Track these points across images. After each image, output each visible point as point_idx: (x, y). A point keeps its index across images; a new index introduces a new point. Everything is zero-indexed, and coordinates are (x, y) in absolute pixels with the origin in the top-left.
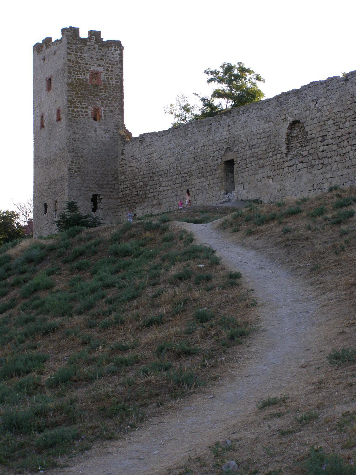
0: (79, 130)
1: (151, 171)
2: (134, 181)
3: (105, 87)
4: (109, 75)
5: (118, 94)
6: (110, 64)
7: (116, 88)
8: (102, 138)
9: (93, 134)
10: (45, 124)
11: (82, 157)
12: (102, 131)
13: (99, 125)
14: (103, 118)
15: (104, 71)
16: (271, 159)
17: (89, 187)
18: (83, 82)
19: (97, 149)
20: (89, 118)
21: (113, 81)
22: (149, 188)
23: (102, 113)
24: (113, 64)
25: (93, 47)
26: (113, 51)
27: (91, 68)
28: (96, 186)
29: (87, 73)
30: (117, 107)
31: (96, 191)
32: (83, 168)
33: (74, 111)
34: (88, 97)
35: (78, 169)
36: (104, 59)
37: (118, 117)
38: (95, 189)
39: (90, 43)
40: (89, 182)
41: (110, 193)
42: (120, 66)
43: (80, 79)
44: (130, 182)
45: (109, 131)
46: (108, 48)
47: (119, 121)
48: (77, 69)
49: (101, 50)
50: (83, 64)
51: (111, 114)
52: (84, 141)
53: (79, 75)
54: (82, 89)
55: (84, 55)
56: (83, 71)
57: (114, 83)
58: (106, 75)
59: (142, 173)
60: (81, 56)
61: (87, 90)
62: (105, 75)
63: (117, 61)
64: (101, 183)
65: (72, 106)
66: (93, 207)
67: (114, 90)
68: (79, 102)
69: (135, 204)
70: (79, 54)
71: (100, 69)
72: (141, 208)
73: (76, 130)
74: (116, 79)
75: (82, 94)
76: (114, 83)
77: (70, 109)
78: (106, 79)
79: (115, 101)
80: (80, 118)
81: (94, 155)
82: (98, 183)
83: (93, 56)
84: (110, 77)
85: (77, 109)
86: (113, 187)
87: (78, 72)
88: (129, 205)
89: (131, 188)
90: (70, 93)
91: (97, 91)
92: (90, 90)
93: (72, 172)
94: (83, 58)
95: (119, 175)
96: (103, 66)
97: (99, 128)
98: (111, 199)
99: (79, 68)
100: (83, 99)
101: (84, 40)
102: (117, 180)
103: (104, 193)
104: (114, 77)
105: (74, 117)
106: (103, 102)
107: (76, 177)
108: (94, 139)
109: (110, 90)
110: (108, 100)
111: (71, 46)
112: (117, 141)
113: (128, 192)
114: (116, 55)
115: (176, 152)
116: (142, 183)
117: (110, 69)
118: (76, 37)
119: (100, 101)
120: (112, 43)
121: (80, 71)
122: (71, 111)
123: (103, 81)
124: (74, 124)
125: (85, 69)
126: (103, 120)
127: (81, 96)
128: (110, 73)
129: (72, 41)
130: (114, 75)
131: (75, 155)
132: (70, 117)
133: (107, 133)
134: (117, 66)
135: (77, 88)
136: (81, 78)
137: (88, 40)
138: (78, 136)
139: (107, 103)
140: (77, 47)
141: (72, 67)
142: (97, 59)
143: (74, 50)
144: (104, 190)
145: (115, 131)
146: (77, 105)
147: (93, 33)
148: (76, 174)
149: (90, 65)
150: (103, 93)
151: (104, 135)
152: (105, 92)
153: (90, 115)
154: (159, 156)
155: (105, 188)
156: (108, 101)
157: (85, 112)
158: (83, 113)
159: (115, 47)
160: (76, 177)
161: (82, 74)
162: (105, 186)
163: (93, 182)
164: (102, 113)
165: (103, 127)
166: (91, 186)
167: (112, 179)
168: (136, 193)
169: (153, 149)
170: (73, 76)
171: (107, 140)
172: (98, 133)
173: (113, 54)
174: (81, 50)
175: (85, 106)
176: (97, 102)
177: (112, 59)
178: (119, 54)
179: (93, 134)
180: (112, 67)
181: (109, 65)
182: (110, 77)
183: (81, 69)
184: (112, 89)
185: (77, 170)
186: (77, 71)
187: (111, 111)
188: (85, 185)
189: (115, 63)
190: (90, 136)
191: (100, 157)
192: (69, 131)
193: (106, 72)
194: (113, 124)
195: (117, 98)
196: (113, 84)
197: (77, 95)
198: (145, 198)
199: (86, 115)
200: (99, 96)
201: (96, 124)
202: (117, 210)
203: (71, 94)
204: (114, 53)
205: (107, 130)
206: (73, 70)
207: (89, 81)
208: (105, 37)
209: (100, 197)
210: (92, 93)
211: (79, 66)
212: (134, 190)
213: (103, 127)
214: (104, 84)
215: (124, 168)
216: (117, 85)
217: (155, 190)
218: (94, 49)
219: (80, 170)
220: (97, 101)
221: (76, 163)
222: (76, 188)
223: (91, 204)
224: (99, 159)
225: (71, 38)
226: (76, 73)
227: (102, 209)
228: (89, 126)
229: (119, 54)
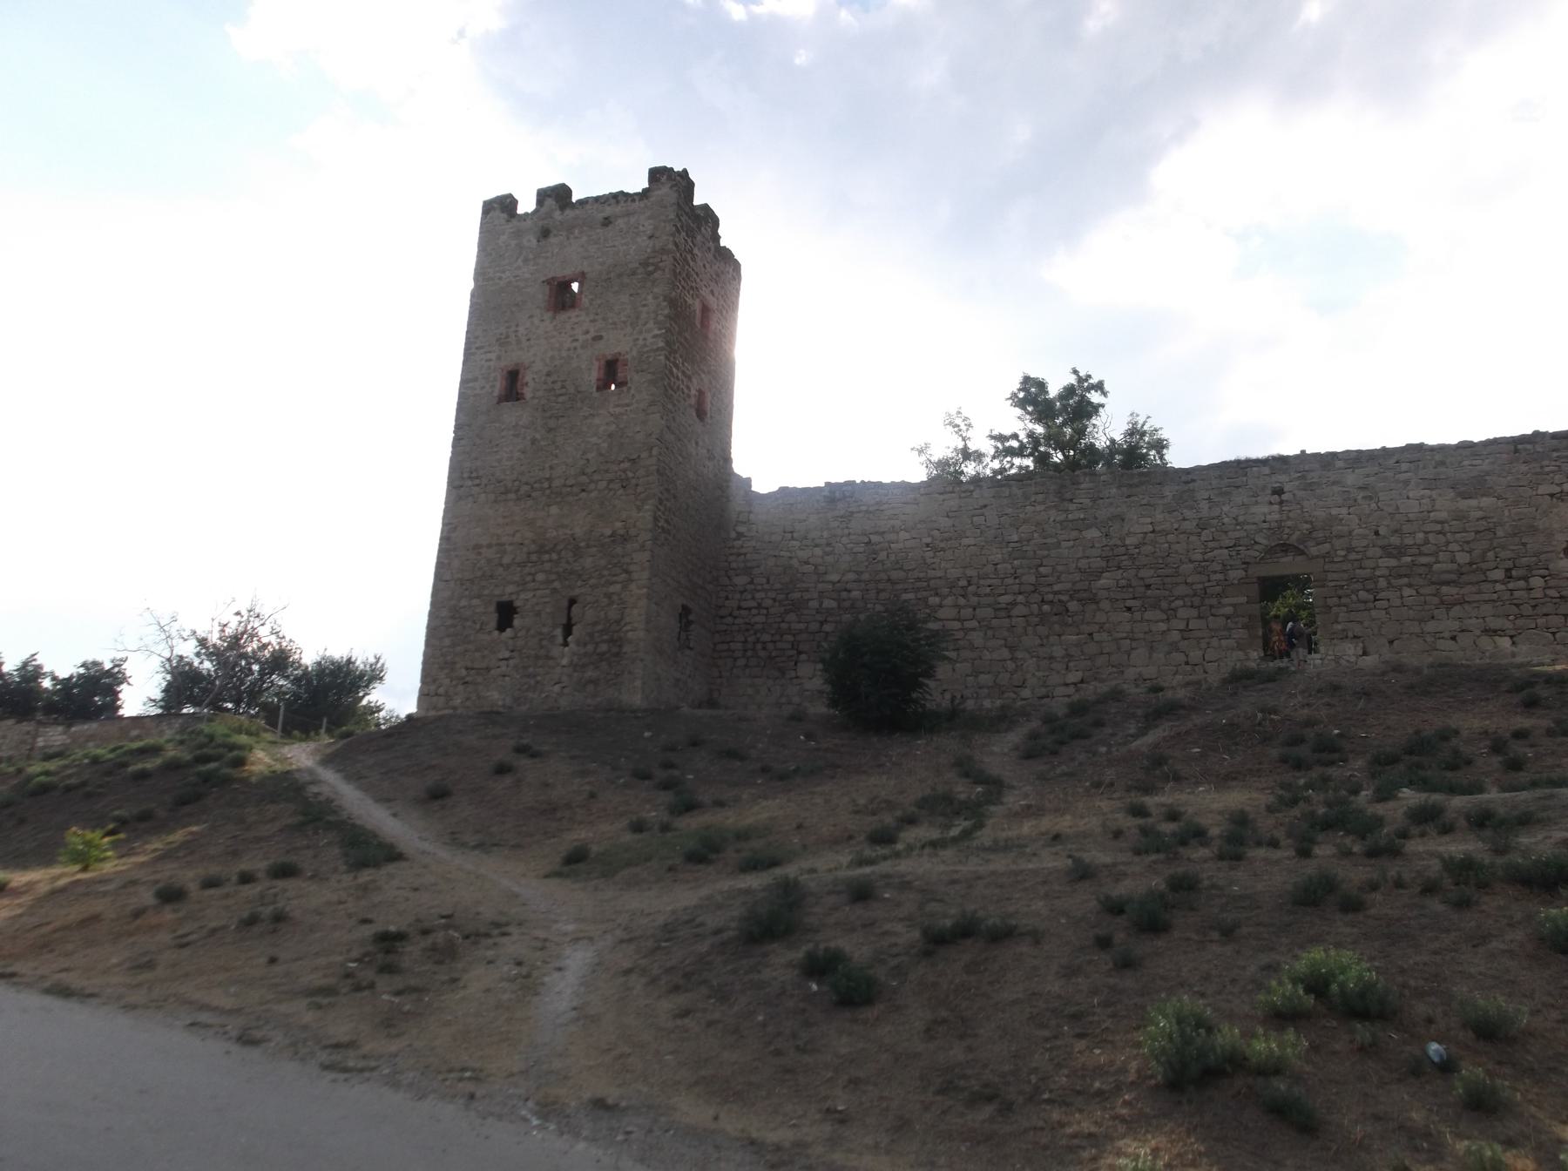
10: (528, 393)
16: (1499, 587)
88: (762, 654)
115: (1015, 538)
154: (929, 540)
212: (792, 617)
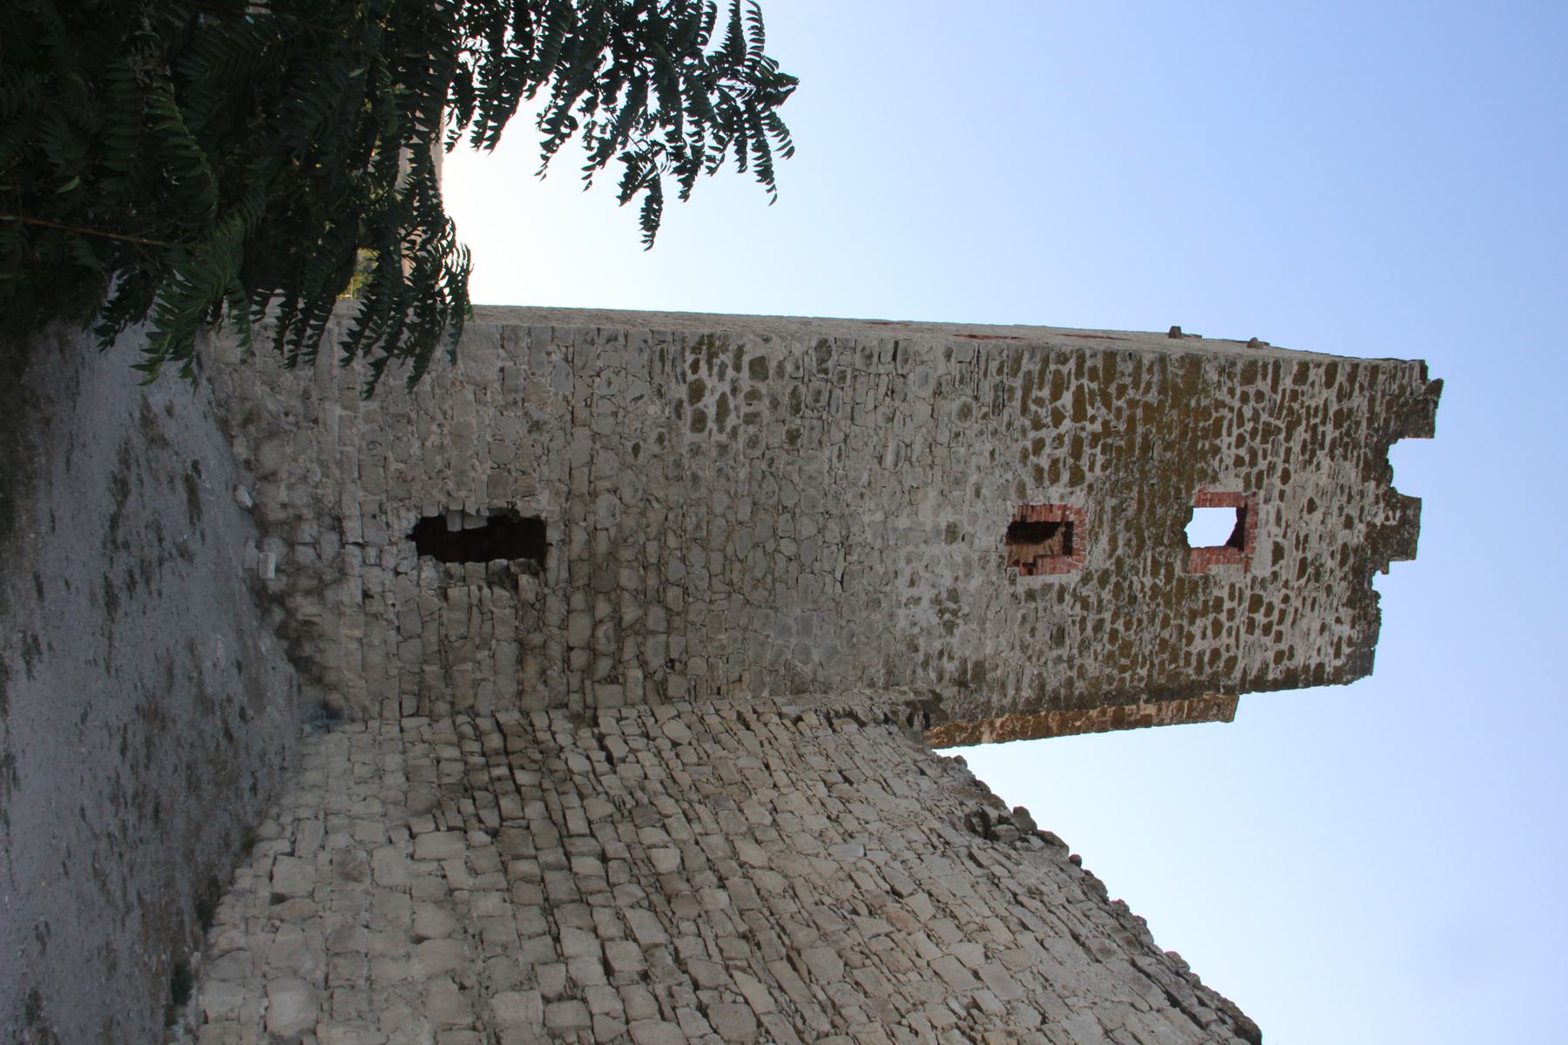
0: (959, 426)
1: (802, 936)
2: (667, 805)
3: (1180, 596)
4: (1231, 614)
5: (1143, 672)
6: (1283, 613)
7: (1174, 659)
8: (912, 583)
9: (930, 514)
11: (793, 436)
12: (947, 582)
13: (984, 560)
14: (1026, 583)
15: (1254, 579)
17: (594, 495)
18: (1203, 455)
19: (845, 546)
20: (1021, 489)
21: (1204, 636)
22: (649, 929)
23: (1049, 579)
24: (1279, 637)
25: (1355, 513)
26: (1336, 628)
27: (1267, 501)
28: (602, 546)
29: (1247, 478)
30: (1082, 673)
31: (566, 541)
32: (723, 449)
33: (1056, 395)
34: (1128, 487)
35: (711, 412)
36: (1303, 581)
37: (1026, 681)
38: (579, 536)
39: (1372, 498)
40: (627, 495)
41: (555, 650)
42: (1271, 677)
43: (1218, 434)
44: (656, 773)
45: (950, 627)
46: (1350, 603)
47: (1003, 686)
48: (1264, 417)
49: (1342, 563)
50: (1287, 460)
51: (1043, 633)
52: (889, 459)
53: (1235, 432)
54: (1168, 446)
55: (1326, 463)
56: (1253, 463)
57: (1198, 645)
58: (1232, 597)
59: (752, 854)
60: (1322, 447)
61: (1165, 479)
62: (1232, 586)
63: (1291, 656)
64: (627, 577)
65: (1085, 381)
66: (454, 526)
67: (1164, 643)
68: (1105, 424)
69: (492, 819)
70: (1330, 432)
71: (1262, 565)
72: (458, 874)
73: (955, 406)
74: (1216, 654)
75: (1147, 447)
76: (1198, 645)
77: (1072, 364)
78: (1216, 592)
79: (1111, 655)
80: (1024, 432)
81: (807, 528)
82: (626, 554)
83: (1318, 515)
84: (1223, 617)
85: (1069, 411)
86: (604, 666)
87: (1249, 426)
89: (609, 780)
90: (1150, 370)
91: (1158, 541)
92: (1164, 499)
93: (695, 367)
94: (1313, 454)
95: (685, 707)
96: (1275, 575)
97: (968, 563)
98: (520, 661)
99: (1269, 432)
100: (1119, 449)
101: (1379, 469)
102: (652, 697)
103: (555, 606)
104: (1225, 638)
105: (1027, 391)
106: (1104, 579)
107: (660, 394)
108: (903, 522)
109: (1165, 623)
110: (1116, 616)
111: (1362, 388)
112: (891, 681)
113: (578, 763)
114: (1310, 651)
116: (667, 860)
117: (1260, 617)
118: (1398, 415)
119: (1109, 565)
120: (1369, 624)
121: (1254, 433)
122: (1058, 372)
123: (1206, 578)
124: (988, 397)
125: (1262, 465)
126: (1013, 582)
127: (1139, 440)
128: (1241, 619)
129: (1383, 392)
130: (1232, 641)
131: (803, 389)
132: (1026, 365)
133: (942, 612)
134: (1270, 655)
135: (1174, 412)
136: (1225, 441)
137: (1383, 488)
138: (923, 410)
139: (1100, 609)
140: (1358, 423)
141: (1274, 389)
142: (1306, 536)
143: (1345, 405)
144: (578, 600)
145: (950, 667)
146: (1090, 412)
147: (1410, 512)
148: (682, 392)
149: (1282, 495)
150: (1148, 581)
151: (927, 594)
152: (1154, 587)
153: (1037, 498)
155: (591, 609)
156: (1107, 616)
157: (1055, 462)
158: (1047, 450)
159: (1350, 642)
160: (660, 394)
161: (1243, 452)
162: (603, 609)
163: (630, 522)
164: (1049, 579)
165: (976, 582)
166: (604, 501)
167: (656, 662)
168: (577, 824)
169: (1000, 933)
170: (1231, 392)
171: (902, 612)
172: (939, 549)
173: (1323, 628)
174: (1345, 445)
175: (1084, 463)
176: (1104, 539)
177: (1303, 624)
178: (1320, 666)
179: (930, 514)
180: (1267, 629)
181: (1276, 614)
182: (1223, 617)
183: (1264, 441)
184: (1166, 634)
185: (709, 403)
186: (1256, 417)
187: (1059, 637)
188: (607, 463)
189: (1283, 646)
190: (920, 494)
191: (793, 566)
192: (948, 355)
193: (1248, 593)
194: (988, 650)
195: (1123, 669)
196: (1190, 638)
197: (1139, 413)
198: (549, 907)
199: (1039, 471)
200: (1137, 555)
201: (990, 536)
202: (442, 707)
203: (1145, 377)
204: (1326, 634)
205: (955, 613)
206: (1260, 396)
207: (1212, 489)
208: (1393, 585)
209: (525, 580)
210: (1153, 506)
211: (1279, 430)
212: (600, 808)
213: (976, 582)
214: (1194, 591)
215: (742, 733)
216: (1188, 664)
217: (640, 999)
218: (1349, 524)
219: (711, 424)
220: (1113, 541)
221: (753, 395)
222: (583, 392)
223: (474, 502)
224: (781, 562)
225: (1395, 386)
226: (1248, 413)
227: (444, 596)
228: (978, 494)
229: (1320, 666)
